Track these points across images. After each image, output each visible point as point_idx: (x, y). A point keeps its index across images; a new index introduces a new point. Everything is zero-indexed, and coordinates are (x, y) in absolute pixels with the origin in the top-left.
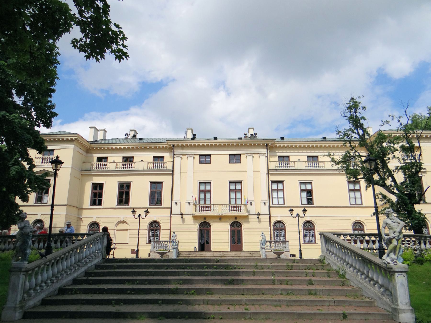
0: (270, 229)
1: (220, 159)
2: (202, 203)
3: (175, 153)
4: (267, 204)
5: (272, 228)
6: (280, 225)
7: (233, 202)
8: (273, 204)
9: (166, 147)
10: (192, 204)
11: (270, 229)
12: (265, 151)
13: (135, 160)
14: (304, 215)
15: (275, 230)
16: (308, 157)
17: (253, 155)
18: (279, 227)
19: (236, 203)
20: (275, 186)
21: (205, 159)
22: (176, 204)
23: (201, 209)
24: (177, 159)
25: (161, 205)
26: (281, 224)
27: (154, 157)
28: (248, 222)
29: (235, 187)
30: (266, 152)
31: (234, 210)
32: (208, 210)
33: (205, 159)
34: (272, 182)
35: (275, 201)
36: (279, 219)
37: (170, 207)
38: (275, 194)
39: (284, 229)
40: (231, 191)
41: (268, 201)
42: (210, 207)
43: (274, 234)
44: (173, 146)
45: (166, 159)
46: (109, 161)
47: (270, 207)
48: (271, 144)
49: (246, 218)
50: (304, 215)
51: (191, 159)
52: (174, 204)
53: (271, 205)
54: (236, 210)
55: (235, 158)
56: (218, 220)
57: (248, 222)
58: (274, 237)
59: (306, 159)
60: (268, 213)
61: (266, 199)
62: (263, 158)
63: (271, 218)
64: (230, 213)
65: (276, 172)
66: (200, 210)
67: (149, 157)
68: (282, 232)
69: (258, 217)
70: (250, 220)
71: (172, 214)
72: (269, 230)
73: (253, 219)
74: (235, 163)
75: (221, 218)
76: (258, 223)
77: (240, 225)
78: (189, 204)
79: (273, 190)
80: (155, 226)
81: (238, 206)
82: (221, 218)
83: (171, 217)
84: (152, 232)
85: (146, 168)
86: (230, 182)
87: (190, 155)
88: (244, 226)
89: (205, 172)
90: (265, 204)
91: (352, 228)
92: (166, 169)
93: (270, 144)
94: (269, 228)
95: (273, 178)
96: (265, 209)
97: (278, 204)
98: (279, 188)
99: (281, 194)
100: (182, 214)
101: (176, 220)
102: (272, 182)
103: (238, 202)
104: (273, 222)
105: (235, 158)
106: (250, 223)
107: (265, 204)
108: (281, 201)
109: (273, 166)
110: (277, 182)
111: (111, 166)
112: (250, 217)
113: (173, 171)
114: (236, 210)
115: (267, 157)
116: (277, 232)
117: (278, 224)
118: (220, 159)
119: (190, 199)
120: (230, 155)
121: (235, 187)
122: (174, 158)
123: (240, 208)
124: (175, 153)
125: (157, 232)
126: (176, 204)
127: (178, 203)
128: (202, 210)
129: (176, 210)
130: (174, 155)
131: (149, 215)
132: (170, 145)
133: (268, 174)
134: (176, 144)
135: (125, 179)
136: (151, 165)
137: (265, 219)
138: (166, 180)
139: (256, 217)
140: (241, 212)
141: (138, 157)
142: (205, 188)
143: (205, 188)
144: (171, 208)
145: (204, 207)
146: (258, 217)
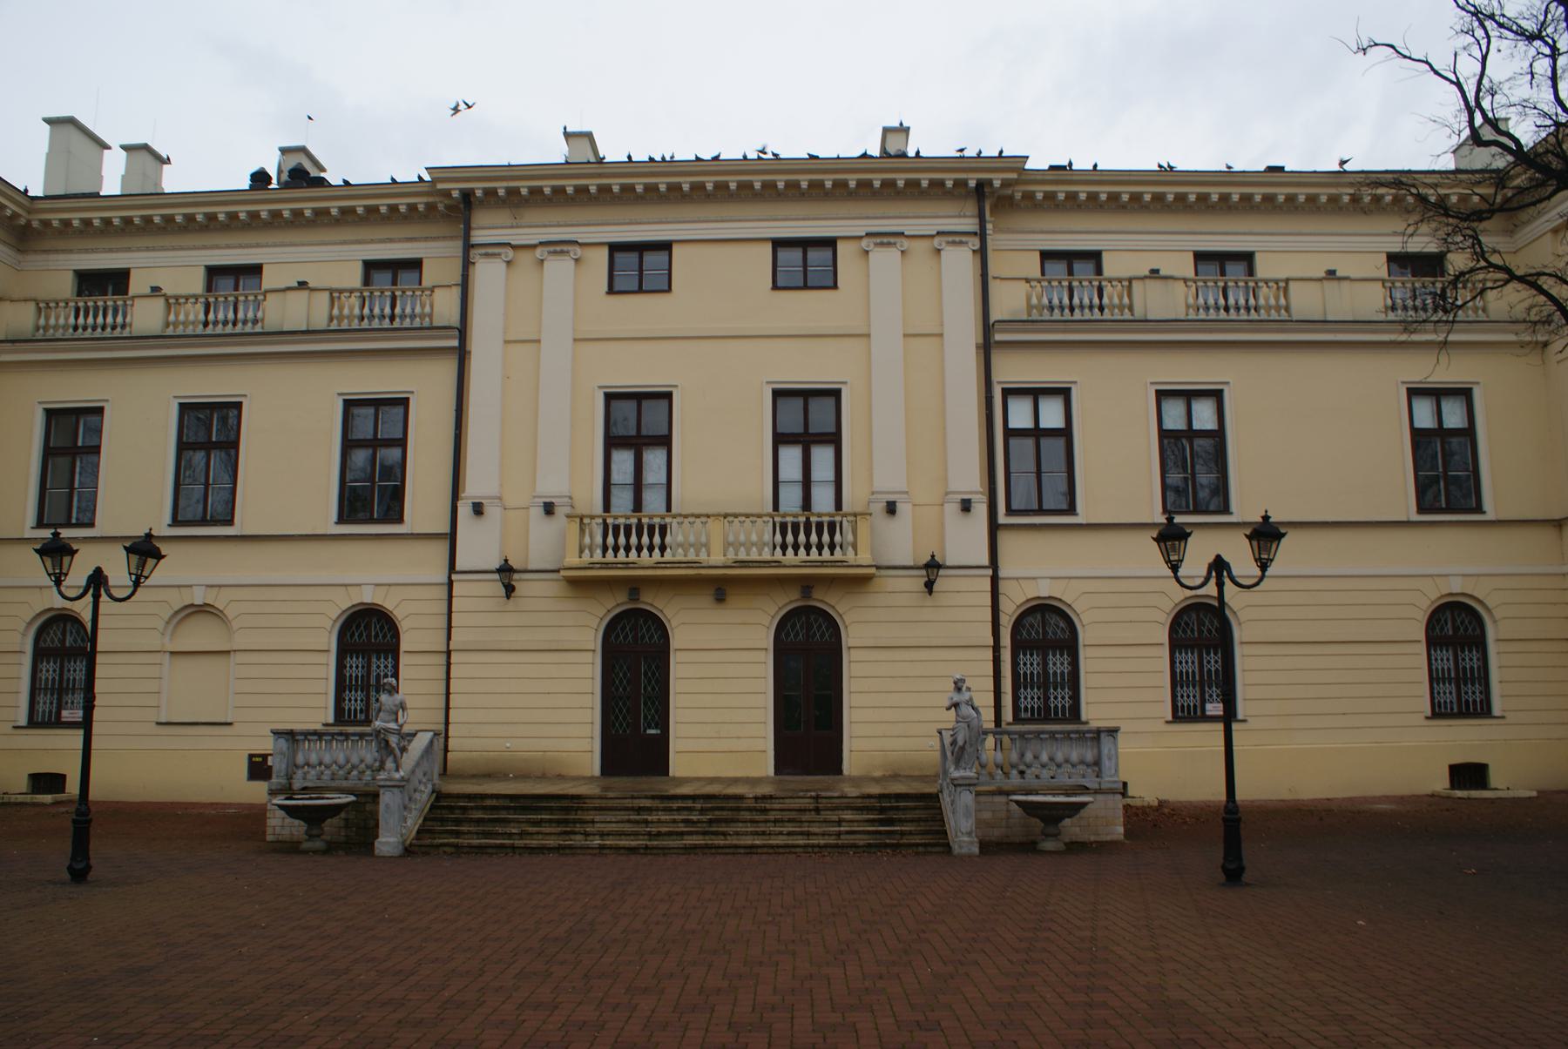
0: (996, 648)
1: (721, 272)
2: (622, 501)
3: (474, 240)
4: (981, 510)
5: (1006, 640)
7: (791, 498)
8: (1010, 511)
9: (431, 207)
10: (560, 511)
11: (996, 648)
12: (970, 224)
13: (269, 279)
14: (1264, 566)
16: (1200, 257)
17: (906, 243)
18: (1043, 641)
19: (807, 503)
20: (1020, 416)
21: (638, 268)
22: (478, 509)
23: (610, 540)
24: (487, 273)
25: (400, 519)
26: (1054, 619)
27: (370, 267)
29: (807, 420)
30: (975, 228)
31: (796, 547)
32: (651, 548)
33: (638, 268)
34: (1007, 393)
36: (1044, 590)
37: (446, 529)
40: (780, 439)
41: (985, 498)
42: (663, 530)
44: (467, 196)
45: (429, 275)
46: (133, 289)
47: (994, 528)
48: (1006, 184)
50: (1264, 566)
51: (559, 269)
52: (464, 510)
53: (1002, 519)
54: (808, 547)
55: (806, 264)
59: (1186, 267)
60: (985, 561)
62: (960, 262)
64: (778, 564)
65: (1034, 332)
66: (605, 549)
67: (336, 263)
71: (458, 568)
74: (806, 287)
75: (721, 587)
78: (549, 509)
79: (1010, 433)
80: (368, 637)
81: (820, 526)
82: (721, 587)
83: (450, 583)
84: (355, 665)
85: (320, 322)
86: (778, 394)
87: (558, 247)
89: (640, 344)
90: (966, 506)
91: (1422, 636)
92: (426, 323)
93: (997, 184)
94: (991, 642)
95: (1012, 370)
96: (966, 541)
97: (1041, 511)
98: (1042, 425)
100: (506, 570)
101: (475, 596)
102: (1007, 393)
103: (823, 500)
105: (806, 264)
109: (1009, 301)
110: (1036, 394)
111: (146, 316)
113: (463, 331)
114: (808, 547)
115: (982, 253)
117: (1035, 620)
118: (721, 272)
119: (552, 485)
120: (778, 244)
121: (807, 420)
122: (467, 264)
123: (832, 535)
124: (478, 236)
125: (380, 665)
126: (478, 509)
127: (487, 509)
128: (616, 549)
129: (480, 546)
130: (468, 246)
131: (160, 574)
132: (447, 194)
133: (987, 348)
134: (479, 187)
135: (209, 385)
136: (352, 305)
138: (426, 387)
139: (916, 582)
140: (838, 554)
141: (283, 262)
142: (637, 424)
143: (637, 424)
144: (452, 537)
145: (628, 529)
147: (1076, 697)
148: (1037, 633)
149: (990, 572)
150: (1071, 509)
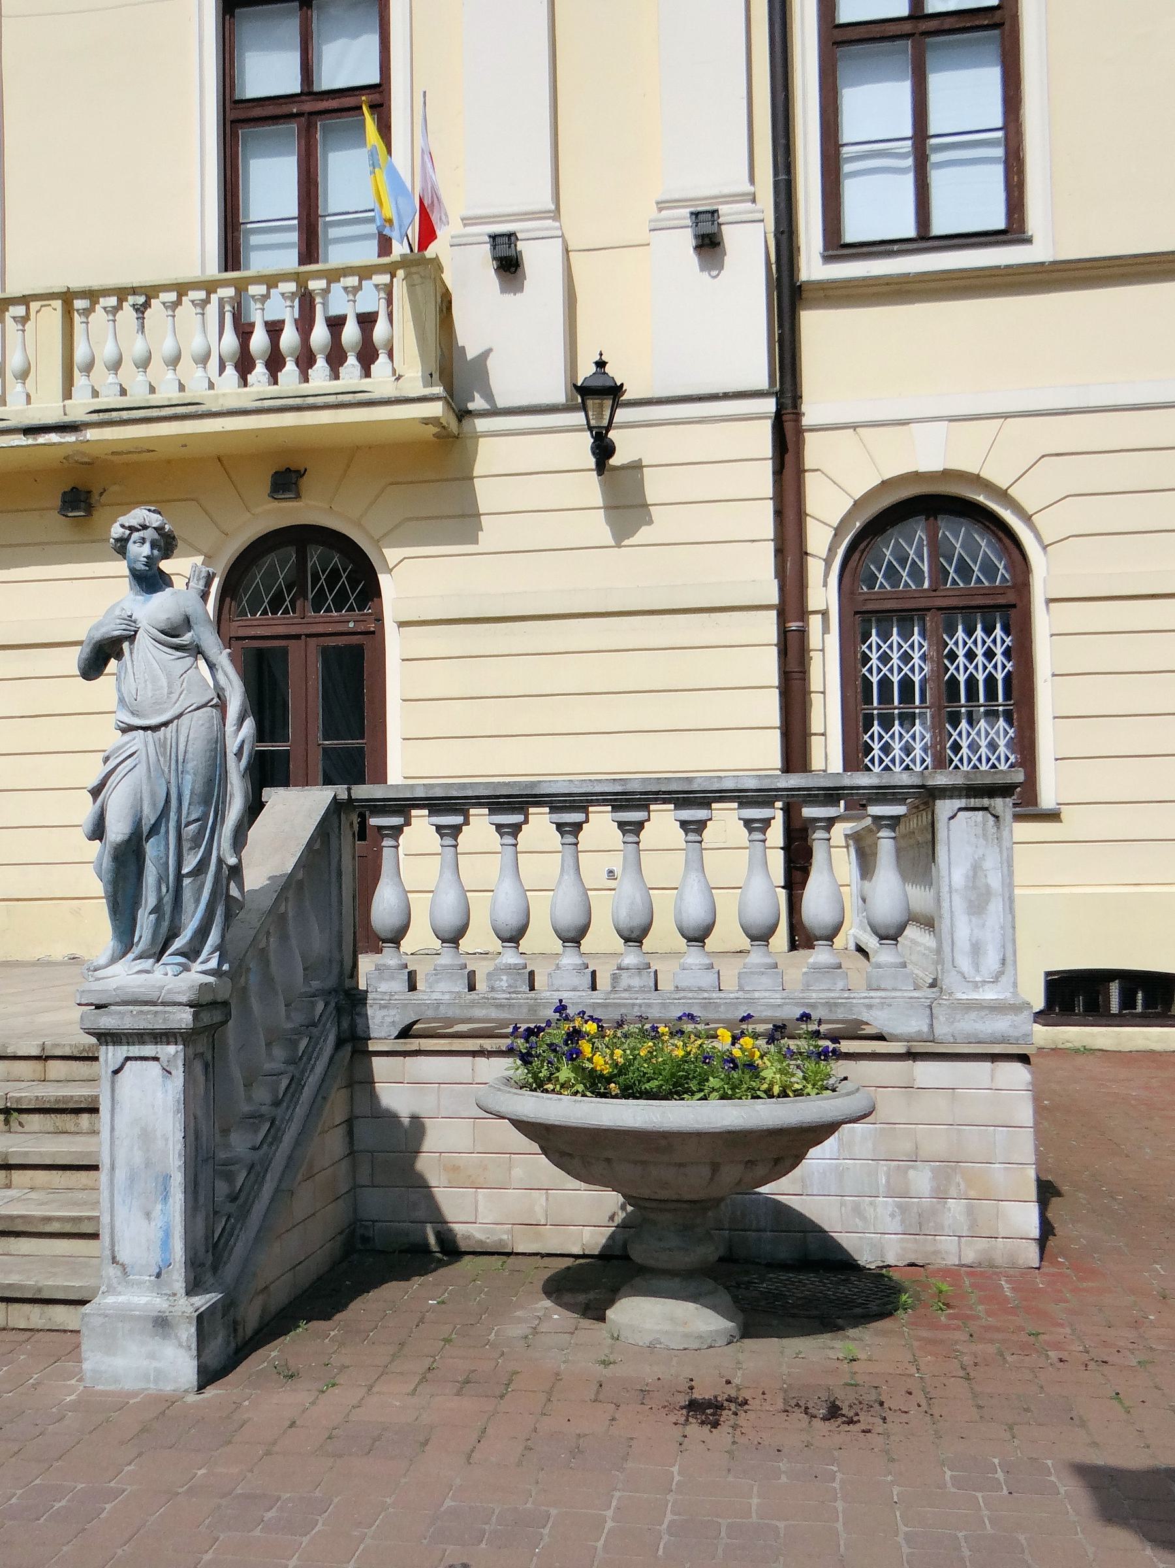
0: (791, 607)
4: (748, 245)
5: (823, 593)
6: (938, 550)
8: (837, 246)
15: (862, 619)
26: (957, 536)
28: (460, 521)
35: (878, 205)
36: (927, 454)
38: (876, 107)
39: (1008, 610)
43: (856, 690)
47: (788, 296)
49: (435, 469)
53: (812, 266)
56: (54, 522)
57: (460, 521)
58: (857, 722)
60: (760, 378)
61: (723, 160)
63: (815, 449)
68: (977, 653)
69: (603, 450)
70: (487, 494)
72: (767, 627)
73: (529, 470)
76: (597, 527)
77: (359, 581)
88: (411, 581)
97: (925, 239)
99: (965, 94)
104: (829, 505)
106: (492, 533)
107: (709, 244)
108: (968, 196)
112: (496, 453)
116: (903, 656)
117: (913, 542)
137: (712, 476)
146: (603, 450)
147: (1025, 747)
148: (916, 573)
149: (769, 405)
150: (1013, 230)
